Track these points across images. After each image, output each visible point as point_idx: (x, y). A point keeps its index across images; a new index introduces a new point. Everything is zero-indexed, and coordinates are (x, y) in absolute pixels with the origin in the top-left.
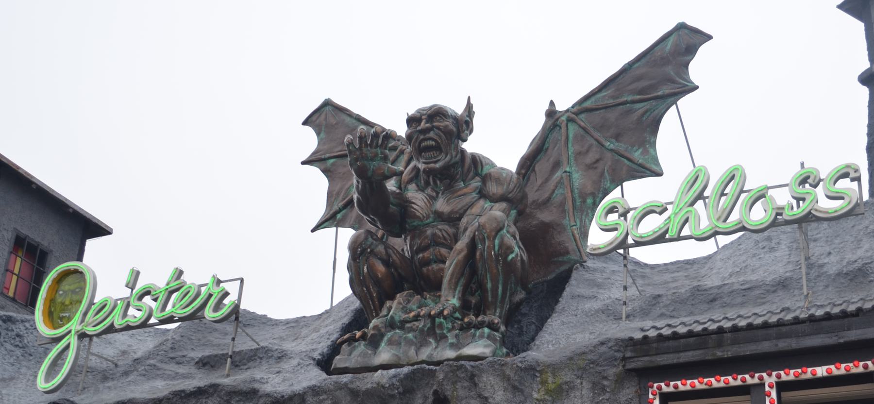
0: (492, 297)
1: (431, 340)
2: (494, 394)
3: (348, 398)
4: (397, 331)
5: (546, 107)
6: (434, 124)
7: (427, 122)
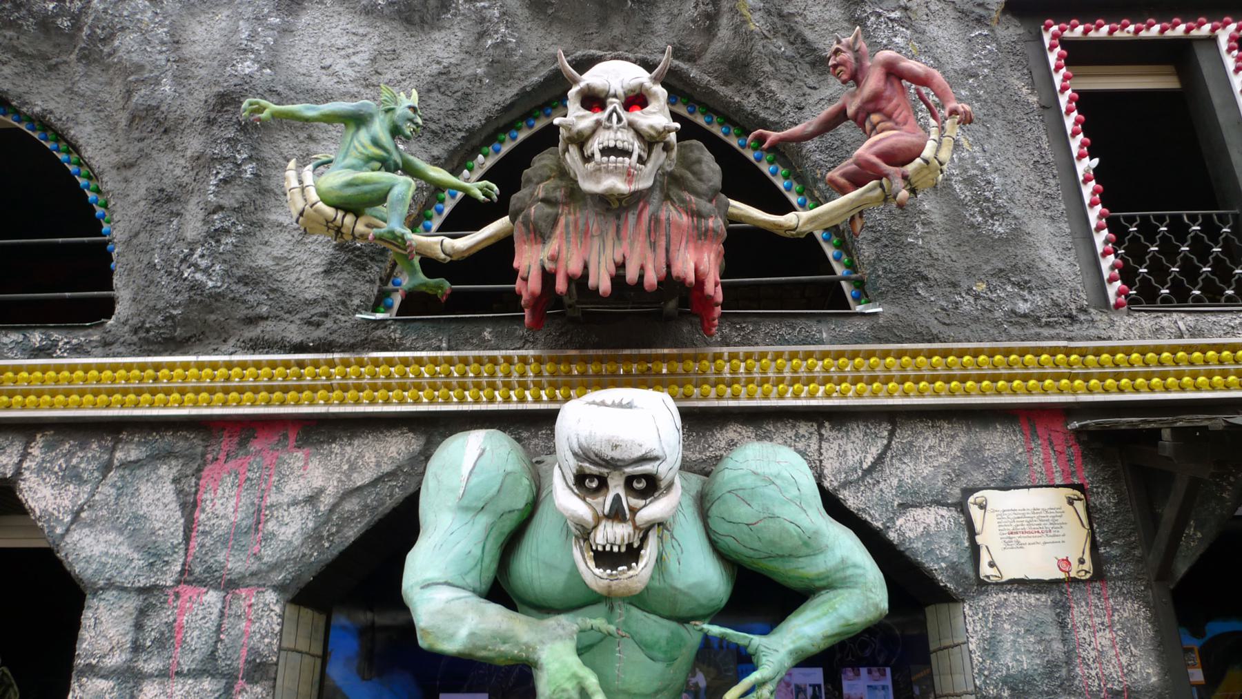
2: (804, 10)
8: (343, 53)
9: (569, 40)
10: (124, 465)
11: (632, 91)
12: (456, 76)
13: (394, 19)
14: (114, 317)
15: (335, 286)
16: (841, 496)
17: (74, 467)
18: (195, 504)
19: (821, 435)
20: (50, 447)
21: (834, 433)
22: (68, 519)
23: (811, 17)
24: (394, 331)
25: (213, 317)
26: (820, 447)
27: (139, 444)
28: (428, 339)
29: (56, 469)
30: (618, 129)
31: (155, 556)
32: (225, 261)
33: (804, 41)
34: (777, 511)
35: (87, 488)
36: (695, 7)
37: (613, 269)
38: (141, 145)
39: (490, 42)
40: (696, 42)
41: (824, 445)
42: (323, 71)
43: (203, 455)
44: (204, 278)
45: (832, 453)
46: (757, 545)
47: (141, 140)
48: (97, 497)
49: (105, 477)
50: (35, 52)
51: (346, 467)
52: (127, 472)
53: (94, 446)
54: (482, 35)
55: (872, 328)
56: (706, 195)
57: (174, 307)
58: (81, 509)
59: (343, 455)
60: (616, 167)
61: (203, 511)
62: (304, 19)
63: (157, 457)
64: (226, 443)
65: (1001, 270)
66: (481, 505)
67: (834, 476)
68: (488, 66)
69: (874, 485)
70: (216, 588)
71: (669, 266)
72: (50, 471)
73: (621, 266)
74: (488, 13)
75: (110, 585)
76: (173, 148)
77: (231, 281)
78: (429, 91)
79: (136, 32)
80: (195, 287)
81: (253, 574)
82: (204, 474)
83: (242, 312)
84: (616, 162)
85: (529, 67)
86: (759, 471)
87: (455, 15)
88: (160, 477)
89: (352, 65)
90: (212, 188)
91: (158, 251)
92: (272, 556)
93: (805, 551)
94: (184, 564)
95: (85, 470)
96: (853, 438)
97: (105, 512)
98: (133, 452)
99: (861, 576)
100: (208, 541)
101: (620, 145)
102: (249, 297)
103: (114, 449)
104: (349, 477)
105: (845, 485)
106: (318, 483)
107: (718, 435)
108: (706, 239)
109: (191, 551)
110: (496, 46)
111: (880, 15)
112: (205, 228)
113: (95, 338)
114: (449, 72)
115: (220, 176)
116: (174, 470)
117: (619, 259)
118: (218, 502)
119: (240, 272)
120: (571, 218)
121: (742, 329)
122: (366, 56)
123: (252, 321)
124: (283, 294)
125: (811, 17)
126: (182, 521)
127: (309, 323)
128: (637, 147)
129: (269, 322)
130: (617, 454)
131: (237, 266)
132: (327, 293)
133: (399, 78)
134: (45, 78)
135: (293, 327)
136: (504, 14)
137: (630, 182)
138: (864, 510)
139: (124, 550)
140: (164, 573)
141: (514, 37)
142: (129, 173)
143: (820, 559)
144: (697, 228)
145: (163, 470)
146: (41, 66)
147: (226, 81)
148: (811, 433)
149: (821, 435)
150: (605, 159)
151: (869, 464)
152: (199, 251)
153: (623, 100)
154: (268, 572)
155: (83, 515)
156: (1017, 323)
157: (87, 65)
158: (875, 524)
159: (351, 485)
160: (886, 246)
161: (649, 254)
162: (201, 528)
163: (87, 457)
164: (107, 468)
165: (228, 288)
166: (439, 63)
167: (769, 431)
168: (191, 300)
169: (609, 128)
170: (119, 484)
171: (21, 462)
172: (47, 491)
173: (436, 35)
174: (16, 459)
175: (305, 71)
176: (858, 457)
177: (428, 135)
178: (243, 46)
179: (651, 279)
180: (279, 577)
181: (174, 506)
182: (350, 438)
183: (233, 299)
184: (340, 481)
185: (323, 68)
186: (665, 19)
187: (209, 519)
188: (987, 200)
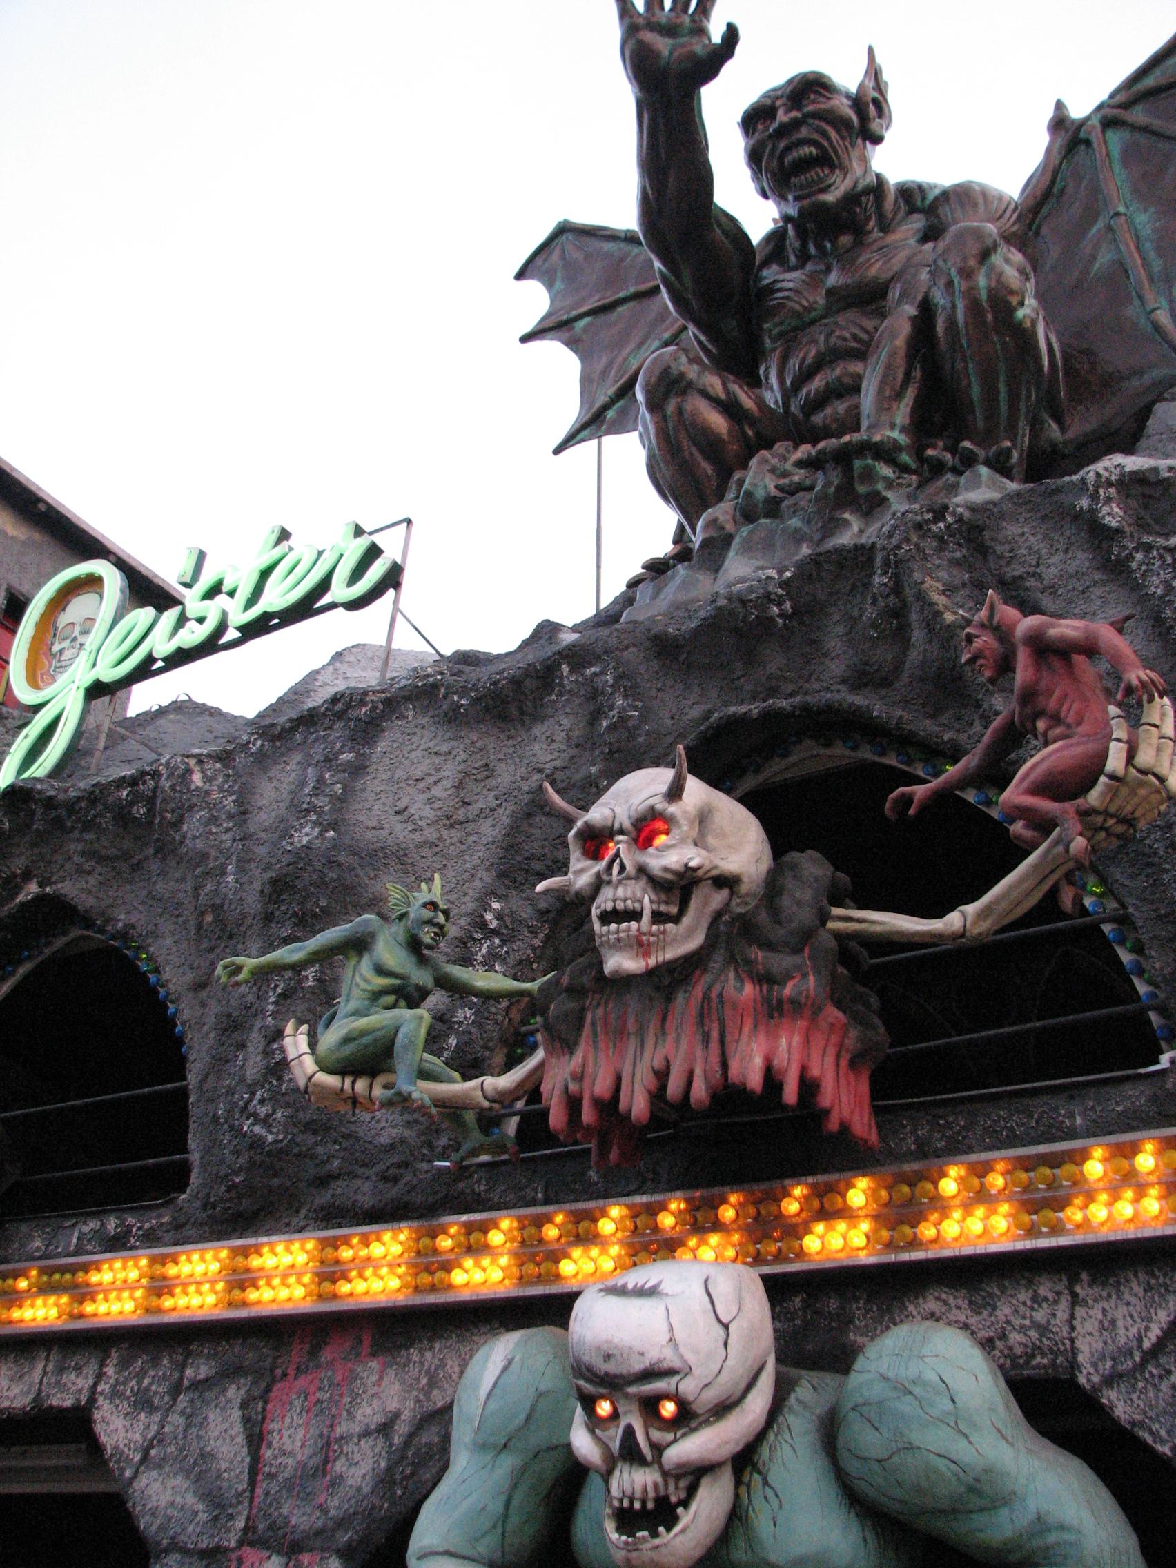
0: (986, 419)
1: (847, 516)
2: (1038, 565)
4: (763, 521)
5: (1049, 113)
6: (810, 108)
7: (787, 111)
8: (421, 785)
9: (714, 693)
10: (197, 1385)
13: (483, 721)
14: (189, 1190)
15: (416, 1121)
16: (1104, 1401)
17: (147, 1389)
18: (261, 1438)
19: (1074, 1295)
20: (124, 1364)
21: (1096, 1290)
22: (137, 1458)
23: (1050, 574)
24: (479, 1181)
25: (276, 1182)
26: (1072, 1316)
27: (208, 1357)
28: (521, 1189)
29: (128, 1393)
30: (620, 882)
31: (219, 1505)
32: (288, 1105)
34: (915, 1437)
35: (157, 1417)
36: (874, 603)
37: (651, 1082)
38: (212, 956)
39: (605, 724)
40: (884, 655)
41: (1080, 1312)
42: (399, 817)
43: (272, 1370)
45: (1092, 1326)
46: (898, 1493)
47: (211, 950)
48: (167, 1429)
49: (175, 1400)
50: (116, 852)
51: (424, 1381)
52: (197, 1394)
53: (165, 1362)
55: (1154, 1099)
56: (786, 944)
58: (151, 1446)
59: (422, 1363)
60: (618, 940)
61: (270, 1445)
62: (382, 746)
63: (229, 1373)
64: (297, 1353)
66: (503, 1442)
67: (1094, 1364)
69: (1161, 1377)
70: (279, 1553)
71: (725, 1065)
72: (122, 1395)
73: (662, 1075)
74: (599, 682)
75: (174, 1547)
77: (296, 1130)
78: (529, 815)
79: (202, 809)
80: (256, 1143)
81: (319, 1533)
82: (272, 1395)
83: (311, 1171)
84: (618, 932)
86: (890, 1374)
87: (560, 695)
88: (229, 1401)
89: (430, 801)
90: (271, 1007)
91: (222, 1099)
92: (339, 1508)
93: (975, 1502)
94: (248, 1519)
95: (156, 1393)
96: (1127, 1296)
97: (173, 1449)
98: (200, 1369)
99: (1071, 1544)
100: (274, 1488)
101: (620, 906)
102: (320, 1150)
103: (182, 1367)
104: (427, 1394)
105: (1110, 1380)
106: (393, 1405)
107: (911, 1308)
108: (781, 1015)
109: (257, 1501)
110: (612, 728)
111: (1148, 548)
113: (166, 1219)
115: (279, 991)
116: (242, 1392)
117: (658, 1063)
118: (286, 1433)
119: (304, 1117)
120: (600, 1012)
121: (949, 1125)
122: (448, 783)
123: (323, 1181)
124: (358, 1139)
125: (1050, 574)
126: (248, 1460)
127: (384, 1178)
129: (339, 1182)
130: (611, 1368)
131: (304, 1109)
132: (407, 1133)
133: (494, 803)
134: (130, 883)
135: (366, 1187)
136: (621, 677)
137: (646, 955)
138: (1141, 1424)
139: (190, 1499)
140: (228, 1531)
141: (636, 708)
142: (203, 995)
143: (1004, 1513)
144: (767, 1001)
145: (231, 1391)
146: (125, 867)
147: (279, 861)
148: (1058, 1293)
149: (1074, 1295)
150: (605, 929)
151: (1154, 1339)
152: (258, 1096)
154: (334, 1530)
155: (153, 1452)
158: (1159, 1447)
159: (429, 1407)
161: (699, 1052)
162: (266, 1469)
163: (156, 1379)
164: (176, 1390)
165: (292, 1140)
167: (991, 1295)
168: (252, 1163)
169: (609, 882)
170: (188, 1410)
171: (95, 1384)
172: (118, 1423)
173: (538, 730)
174: (91, 1382)
175: (374, 823)
176: (1134, 1330)
178: (305, 806)
179: (699, 1091)
180: (344, 1538)
181: (240, 1439)
182: (431, 1340)
184: (418, 1401)
185: (397, 813)
186: (840, 629)
187: (275, 1457)
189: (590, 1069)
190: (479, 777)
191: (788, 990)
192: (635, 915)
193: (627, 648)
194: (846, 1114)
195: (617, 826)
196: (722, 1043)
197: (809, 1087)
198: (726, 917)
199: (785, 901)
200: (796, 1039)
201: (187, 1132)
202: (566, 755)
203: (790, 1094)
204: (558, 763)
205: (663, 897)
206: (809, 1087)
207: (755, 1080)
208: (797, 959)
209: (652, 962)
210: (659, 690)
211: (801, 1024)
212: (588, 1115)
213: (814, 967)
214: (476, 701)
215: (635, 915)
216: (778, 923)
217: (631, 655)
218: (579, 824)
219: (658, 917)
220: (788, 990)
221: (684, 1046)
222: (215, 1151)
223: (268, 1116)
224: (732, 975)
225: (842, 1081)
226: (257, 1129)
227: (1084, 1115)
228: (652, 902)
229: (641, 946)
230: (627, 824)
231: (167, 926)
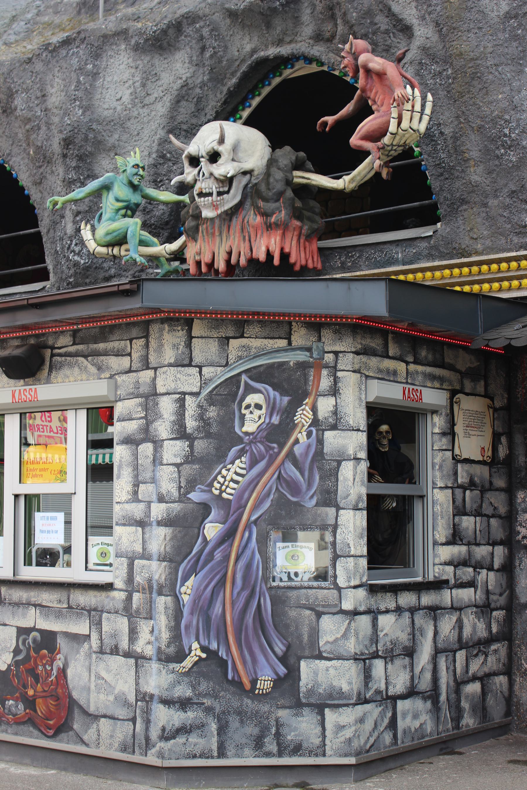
3: (228, 21)
8: (127, 85)
9: (256, 38)
11: (210, 152)
12: (192, 85)
33: (394, 15)
42: (118, 102)
44: (79, 259)
47: (40, 167)
54: (203, 49)
56: (272, 199)
57: (70, 277)
65: (513, 192)
68: (209, 73)
73: (230, 253)
76: (53, 172)
78: (178, 102)
80: (76, 264)
85: (233, 69)
91: (58, 242)
108: (271, 229)
110: (211, 57)
112: (74, 226)
114: (188, 84)
117: (227, 249)
120: (204, 226)
121: (352, 256)
128: (214, 188)
133: (162, 94)
137: (217, 209)
144: (266, 223)
147: (65, 130)
152: (74, 243)
153: (208, 158)
156: (520, 233)
157: (7, 116)
160: (447, 179)
165: (92, 262)
166: (181, 78)
168: (76, 273)
177: (183, 133)
179: (243, 261)
183: (96, 268)
185: (117, 100)
186: (308, 11)
188: (505, 135)
189: (203, 251)
190: (153, 80)
191: (273, 219)
192: (210, 194)
193: (214, 14)
194: (303, 262)
195: (200, 155)
196: (250, 241)
197: (285, 256)
198: (250, 185)
199: (271, 180)
200: (278, 238)
201: (44, 256)
202: (191, 70)
203: (276, 261)
204: (188, 75)
205: (221, 185)
206: (285, 256)
207: (262, 257)
208: (277, 204)
209: (219, 212)
210: (231, 35)
211: (279, 232)
212: (204, 269)
213: (284, 207)
214: (147, 40)
215: (210, 194)
216: (269, 189)
217: (217, 17)
218: (186, 153)
219: (220, 194)
220: (273, 219)
221: (236, 242)
222: (59, 267)
223: (80, 252)
224: (252, 212)
225: (302, 249)
226: (76, 258)
227: (402, 252)
228: (216, 188)
229: (215, 207)
230: (204, 154)
231: (15, 150)
